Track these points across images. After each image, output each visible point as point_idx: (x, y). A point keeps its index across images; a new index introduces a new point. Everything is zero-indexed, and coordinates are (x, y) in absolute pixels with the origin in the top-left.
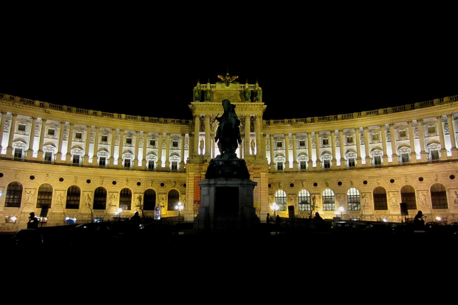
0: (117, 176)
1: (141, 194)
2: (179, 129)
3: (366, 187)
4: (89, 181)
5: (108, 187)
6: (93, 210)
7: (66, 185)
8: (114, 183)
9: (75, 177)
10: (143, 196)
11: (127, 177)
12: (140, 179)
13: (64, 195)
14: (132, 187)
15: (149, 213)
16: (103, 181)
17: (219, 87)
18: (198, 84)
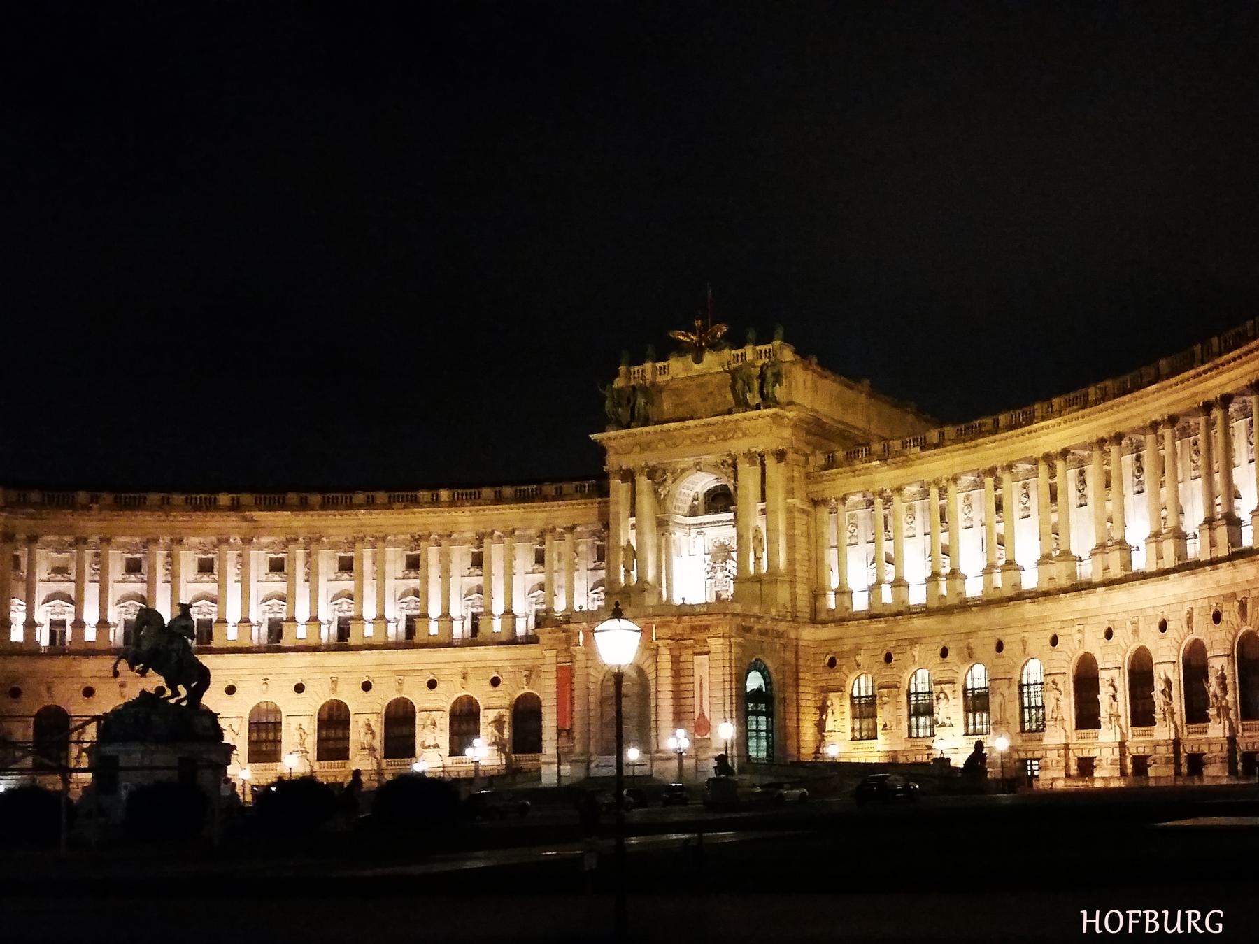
0: (438, 666)
1: (503, 711)
2: (596, 511)
3: (1055, 656)
4: (367, 687)
5: (419, 697)
6: (384, 761)
7: (313, 701)
8: (432, 685)
9: (334, 678)
10: (507, 714)
11: (461, 665)
12: (497, 669)
13: (311, 726)
14: (480, 692)
15: (526, 761)
16: (400, 683)
17: (678, 367)
18: (622, 369)
